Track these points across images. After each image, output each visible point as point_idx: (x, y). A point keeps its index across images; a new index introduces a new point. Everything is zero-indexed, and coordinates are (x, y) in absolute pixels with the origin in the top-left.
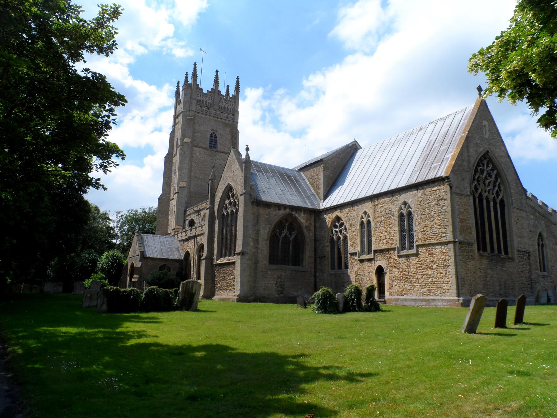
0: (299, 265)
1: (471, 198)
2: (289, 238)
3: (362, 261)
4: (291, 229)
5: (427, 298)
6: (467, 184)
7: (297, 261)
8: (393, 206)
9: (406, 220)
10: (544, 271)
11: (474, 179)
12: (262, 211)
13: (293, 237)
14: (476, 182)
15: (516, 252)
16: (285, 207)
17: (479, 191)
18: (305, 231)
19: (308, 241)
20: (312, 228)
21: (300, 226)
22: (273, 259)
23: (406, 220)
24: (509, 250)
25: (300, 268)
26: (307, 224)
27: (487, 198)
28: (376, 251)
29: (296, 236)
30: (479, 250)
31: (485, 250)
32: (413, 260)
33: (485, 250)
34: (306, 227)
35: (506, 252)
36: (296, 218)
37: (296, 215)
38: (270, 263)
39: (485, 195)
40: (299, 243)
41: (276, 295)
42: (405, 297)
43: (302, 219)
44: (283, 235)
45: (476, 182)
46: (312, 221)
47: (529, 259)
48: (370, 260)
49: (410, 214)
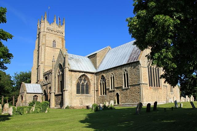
0: (88, 94)
1: (147, 68)
2: (84, 84)
3: (111, 92)
4: (85, 80)
5: (133, 103)
6: (146, 64)
7: (87, 92)
8: (122, 71)
9: (126, 76)
10: (172, 92)
11: (148, 61)
12: (73, 73)
13: (86, 83)
14: (149, 62)
15: (163, 86)
16: (82, 72)
17: (150, 65)
18: (90, 81)
19: (92, 84)
20: (93, 79)
21: (88, 79)
22: (78, 92)
23: (126, 76)
24: (160, 85)
25: (89, 95)
26: (91, 78)
27: (153, 68)
28: (116, 88)
29: (87, 83)
30: (150, 86)
31: (152, 86)
32: (128, 91)
33: (152, 86)
34: (91, 79)
35: (159, 86)
36: (86, 76)
37: (87, 75)
38: (77, 94)
39: (152, 67)
40: (88, 86)
41: (80, 106)
42: (126, 104)
43: (89, 76)
44: (82, 83)
45: (149, 62)
46: (93, 77)
47: (167, 88)
48: (114, 91)
49: (127, 74)
